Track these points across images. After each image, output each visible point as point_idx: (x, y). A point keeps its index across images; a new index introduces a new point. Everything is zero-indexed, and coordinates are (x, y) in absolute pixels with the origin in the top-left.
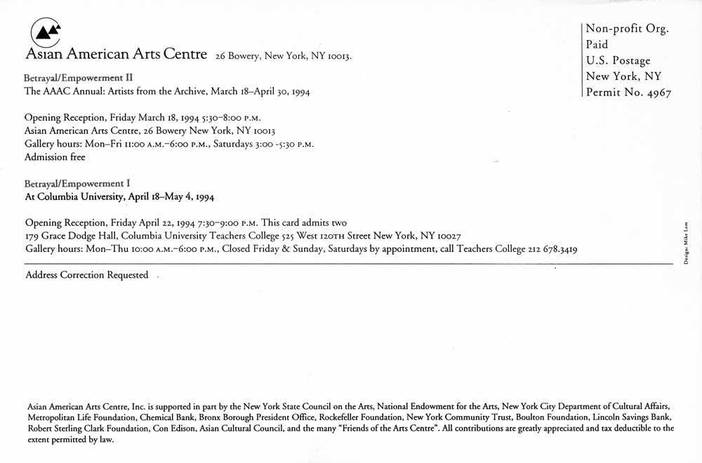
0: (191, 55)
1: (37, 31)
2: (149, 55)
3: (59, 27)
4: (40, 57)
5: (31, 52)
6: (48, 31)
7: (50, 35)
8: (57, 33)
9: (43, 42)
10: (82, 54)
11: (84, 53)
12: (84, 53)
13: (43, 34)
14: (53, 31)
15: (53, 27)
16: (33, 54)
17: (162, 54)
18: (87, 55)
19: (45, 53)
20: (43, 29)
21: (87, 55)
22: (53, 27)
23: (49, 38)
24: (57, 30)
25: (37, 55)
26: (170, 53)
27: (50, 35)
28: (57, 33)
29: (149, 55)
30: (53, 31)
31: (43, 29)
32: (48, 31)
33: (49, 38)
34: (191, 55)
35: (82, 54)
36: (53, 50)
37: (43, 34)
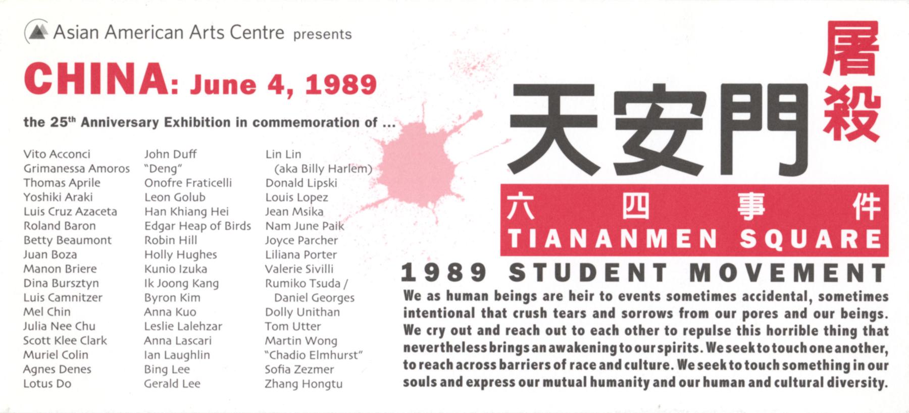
0: (263, 32)
2: (209, 33)
4: (71, 36)
10: (123, 33)
11: (126, 31)
12: (126, 31)
16: (62, 33)
17: (227, 33)
18: (129, 33)
19: (77, 30)
21: (129, 33)
25: (67, 35)
26: (238, 32)
29: (209, 33)
34: (263, 32)
35: (123, 33)
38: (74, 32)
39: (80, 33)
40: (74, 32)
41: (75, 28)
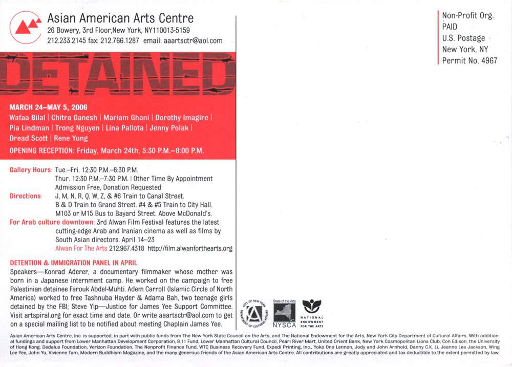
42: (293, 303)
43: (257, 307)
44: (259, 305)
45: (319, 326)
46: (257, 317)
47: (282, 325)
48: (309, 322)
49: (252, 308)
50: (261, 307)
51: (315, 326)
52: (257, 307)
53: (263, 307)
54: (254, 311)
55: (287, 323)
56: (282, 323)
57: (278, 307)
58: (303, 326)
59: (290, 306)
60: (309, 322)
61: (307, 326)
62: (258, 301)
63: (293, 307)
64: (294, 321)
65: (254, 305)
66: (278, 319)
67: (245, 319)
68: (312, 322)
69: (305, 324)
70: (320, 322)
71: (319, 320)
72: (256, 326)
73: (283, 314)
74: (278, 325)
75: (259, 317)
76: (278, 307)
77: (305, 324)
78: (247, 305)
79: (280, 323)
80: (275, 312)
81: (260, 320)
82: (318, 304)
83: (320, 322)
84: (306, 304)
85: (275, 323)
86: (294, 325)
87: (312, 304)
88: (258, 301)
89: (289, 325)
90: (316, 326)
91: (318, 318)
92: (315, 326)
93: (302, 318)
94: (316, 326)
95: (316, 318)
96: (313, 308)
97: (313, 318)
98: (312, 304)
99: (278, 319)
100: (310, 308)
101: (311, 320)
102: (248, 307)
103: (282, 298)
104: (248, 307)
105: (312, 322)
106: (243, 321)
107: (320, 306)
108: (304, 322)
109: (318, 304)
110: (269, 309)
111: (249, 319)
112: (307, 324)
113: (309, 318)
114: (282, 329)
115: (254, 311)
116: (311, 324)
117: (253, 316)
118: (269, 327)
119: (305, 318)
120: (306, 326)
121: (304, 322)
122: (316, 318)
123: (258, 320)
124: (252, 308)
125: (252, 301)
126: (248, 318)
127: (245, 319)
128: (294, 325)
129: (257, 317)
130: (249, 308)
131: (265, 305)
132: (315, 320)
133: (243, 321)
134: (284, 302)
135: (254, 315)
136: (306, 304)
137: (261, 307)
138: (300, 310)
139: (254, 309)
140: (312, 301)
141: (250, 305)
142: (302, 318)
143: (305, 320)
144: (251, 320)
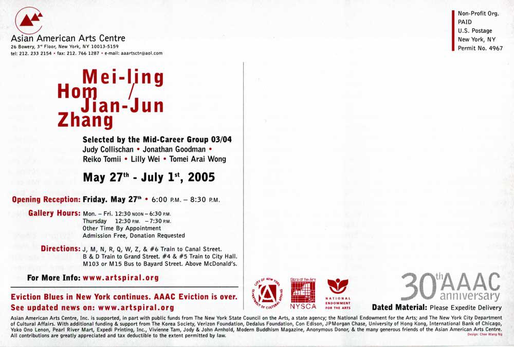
1: (21, 19)
3: (40, 15)
5: (14, 38)
6: (31, 17)
7: (33, 22)
8: (38, 20)
9: (27, 29)
13: (26, 22)
14: (35, 18)
15: (35, 15)
16: (16, 40)
20: (27, 17)
22: (35, 15)
23: (32, 25)
24: (39, 18)
25: (17, 40)
27: (33, 22)
28: (38, 20)
30: (35, 18)
31: (27, 17)
32: (31, 17)
33: (32, 25)
36: (28, 36)
37: (26, 22)
38: (21, 38)
39: (24, 38)
40: (21, 38)
41: (21, 37)
42: (313, 280)
43: (270, 286)
44: (273, 283)
45: (345, 308)
46: (270, 297)
47: (300, 307)
48: (335, 303)
49: (264, 288)
50: (275, 286)
51: (341, 308)
52: (270, 286)
53: (277, 286)
54: (267, 291)
55: (305, 304)
56: (301, 303)
57: (296, 286)
58: (329, 308)
59: (309, 284)
60: (335, 303)
61: (333, 308)
62: (272, 280)
63: (313, 285)
64: (314, 302)
65: (267, 284)
66: (296, 299)
67: (257, 300)
68: (338, 303)
69: (330, 306)
70: (347, 303)
71: (345, 301)
72: (270, 308)
73: (302, 294)
74: (296, 306)
75: (272, 298)
76: (296, 286)
77: (330, 306)
78: (260, 284)
79: (298, 303)
80: (292, 291)
81: (274, 299)
82: (345, 283)
83: (347, 303)
84: (331, 283)
85: (293, 304)
86: (314, 306)
87: (338, 284)
88: (272, 280)
89: (308, 306)
90: (343, 308)
91: (345, 298)
92: (341, 308)
93: (327, 298)
94: (343, 308)
95: (343, 298)
96: (340, 287)
97: (339, 298)
98: (338, 284)
99: (296, 299)
100: (336, 287)
101: (338, 301)
102: (260, 286)
103: (299, 276)
104: (260, 286)
105: (338, 303)
106: (255, 301)
107: (347, 286)
108: (329, 303)
109: (345, 283)
110: (285, 289)
111: (261, 300)
112: (333, 306)
113: (335, 298)
114: (301, 310)
115: (267, 291)
116: (338, 306)
117: (265, 297)
118: (285, 307)
119: (330, 298)
120: (331, 308)
121: (329, 303)
122: (343, 298)
123: (271, 301)
124: (264, 288)
125: (265, 279)
126: (260, 298)
127: (257, 300)
128: (314, 306)
129: (270, 297)
130: (261, 287)
131: (280, 283)
132: (341, 301)
133: (255, 301)
134: (303, 280)
135: (267, 295)
136: (331, 283)
137: (275, 286)
138: (323, 291)
139: (268, 288)
140: (338, 280)
141: (263, 284)
142: (327, 298)
143: (329, 301)
144: (264, 301)
